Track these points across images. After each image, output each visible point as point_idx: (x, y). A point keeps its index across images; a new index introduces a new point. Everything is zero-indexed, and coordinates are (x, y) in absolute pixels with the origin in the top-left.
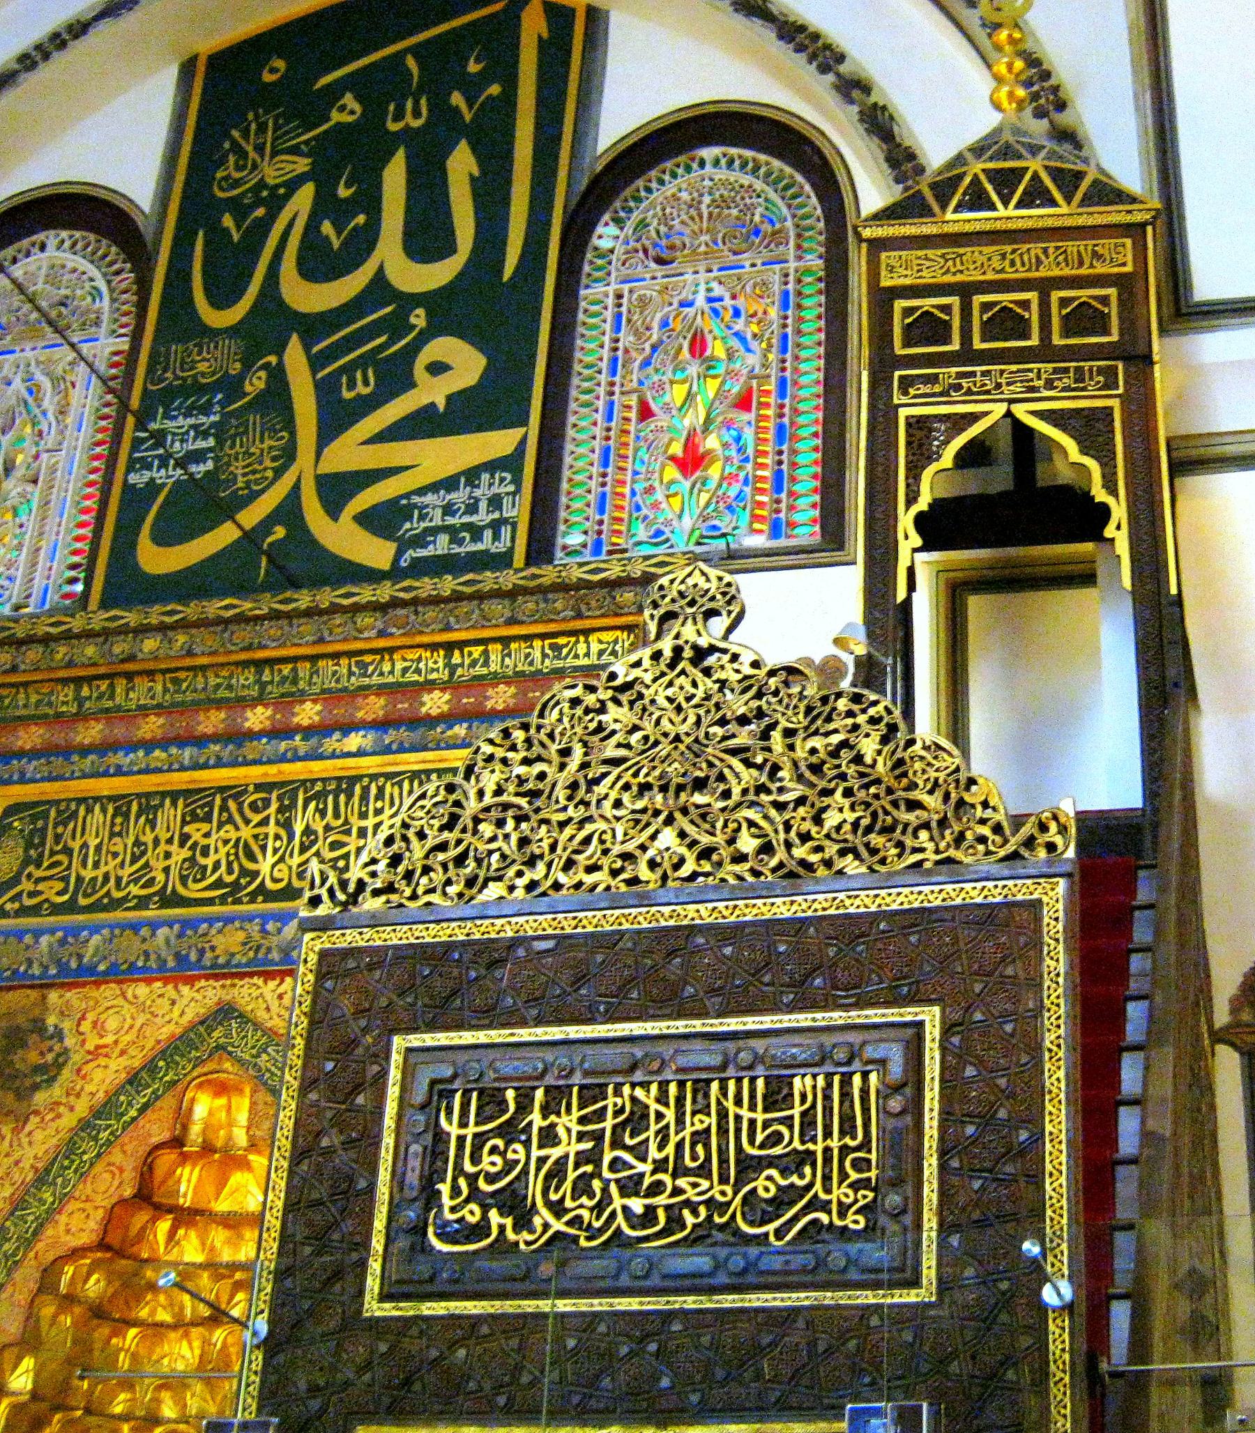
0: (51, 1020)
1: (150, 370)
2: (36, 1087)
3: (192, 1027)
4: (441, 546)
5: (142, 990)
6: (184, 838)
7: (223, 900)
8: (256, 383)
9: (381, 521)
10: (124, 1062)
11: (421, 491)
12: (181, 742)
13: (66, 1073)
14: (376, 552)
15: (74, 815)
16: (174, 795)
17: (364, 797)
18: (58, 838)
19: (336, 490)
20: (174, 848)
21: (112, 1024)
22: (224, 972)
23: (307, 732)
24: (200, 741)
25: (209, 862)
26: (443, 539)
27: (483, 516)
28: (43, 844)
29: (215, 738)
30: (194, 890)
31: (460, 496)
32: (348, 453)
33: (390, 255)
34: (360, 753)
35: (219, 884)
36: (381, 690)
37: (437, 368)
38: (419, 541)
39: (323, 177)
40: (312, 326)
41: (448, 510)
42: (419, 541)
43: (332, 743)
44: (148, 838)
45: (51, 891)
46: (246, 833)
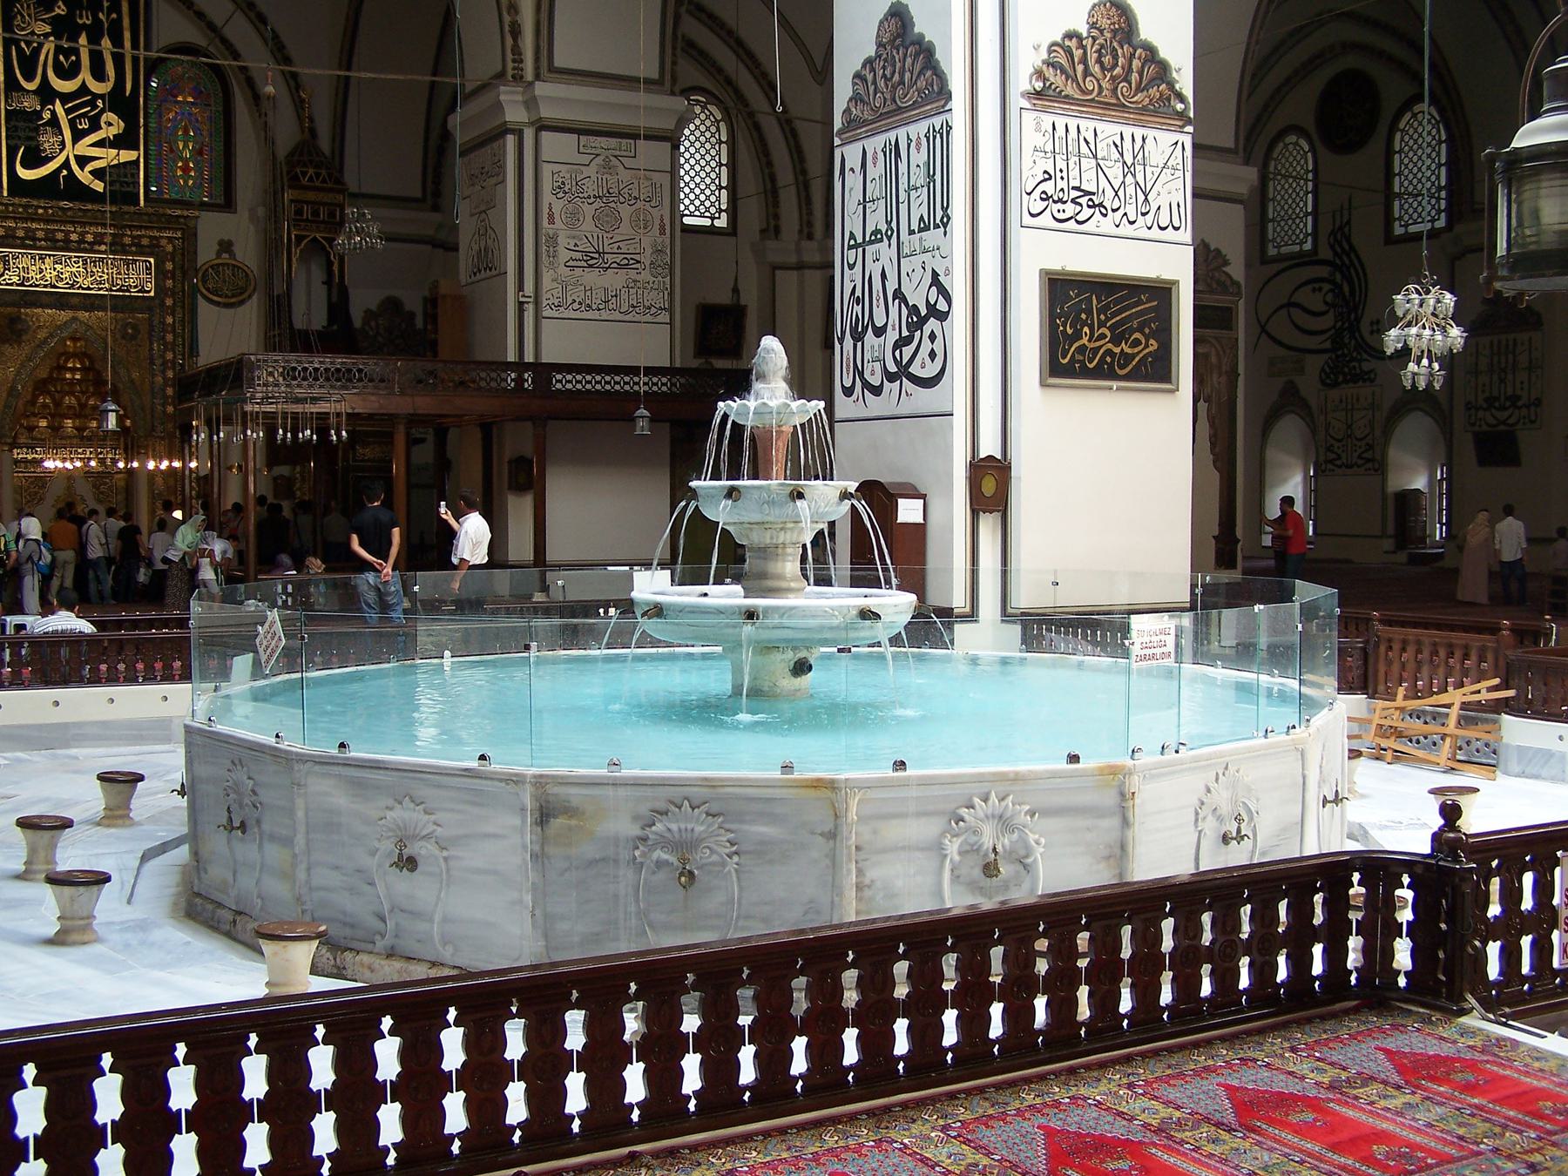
9: (98, 174)
14: (99, 186)
19: (83, 161)
22: (73, 308)
32: (83, 147)
33: (85, 75)
37: (110, 124)
39: (57, 34)
40: (65, 98)
45: (15, 279)
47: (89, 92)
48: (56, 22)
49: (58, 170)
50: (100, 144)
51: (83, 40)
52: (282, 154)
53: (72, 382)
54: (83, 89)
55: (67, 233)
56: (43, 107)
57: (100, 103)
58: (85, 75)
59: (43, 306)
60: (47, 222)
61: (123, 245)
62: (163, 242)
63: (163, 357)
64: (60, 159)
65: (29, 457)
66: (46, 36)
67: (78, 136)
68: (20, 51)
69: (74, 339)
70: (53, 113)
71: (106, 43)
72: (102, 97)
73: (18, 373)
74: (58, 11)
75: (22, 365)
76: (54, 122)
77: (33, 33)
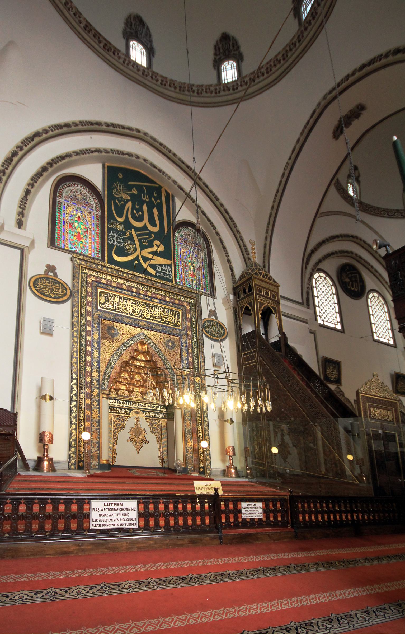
0: (115, 327)
1: (108, 223)
2: (114, 336)
3: (138, 334)
4: (162, 274)
5: (129, 326)
6: (132, 306)
7: (139, 317)
8: (128, 235)
10: (128, 336)
11: (158, 265)
12: (130, 291)
13: (119, 336)
15: (113, 296)
16: (129, 299)
17: (158, 309)
18: (111, 299)
20: (130, 307)
21: (125, 330)
22: (141, 327)
23: (149, 297)
24: (133, 292)
25: (136, 311)
26: (162, 274)
27: (167, 272)
28: (108, 299)
29: (135, 292)
30: (134, 314)
31: (164, 268)
34: (157, 302)
35: (138, 314)
36: (160, 295)
38: (159, 272)
40: (137, 229)
41: (162, 269)
42: (159, 272)
43: (153, 300)
44: (126, 304)
45: (111, 307)
46: (142, 308)
47: (148, 230)
48: (132, 195)
49: (133, 261)
50: (155, 253)
51: (145, 207)
52: (237, 276)
53: (140, 368)
54: (145, 228)
55: (138, 289)
56: (126, 229)
57: (153, 235)
58: (146, 221)
59: (125, 323)
60: (128, 281)
61: (165, 301)
62: (185, 304)
63: (188, 360)
64: (135, 255)
65: (116, 405)
66: (128, 201)
67: (143, 247)
68: (116, 204)
69: (143, 344)
70: (131, 234)
71: (155, 211)
72: (154, 233)
73: (112, 356)
74: (133, 192)
75: (114, 353)
76: (131, 238)
77: (122, 197)
